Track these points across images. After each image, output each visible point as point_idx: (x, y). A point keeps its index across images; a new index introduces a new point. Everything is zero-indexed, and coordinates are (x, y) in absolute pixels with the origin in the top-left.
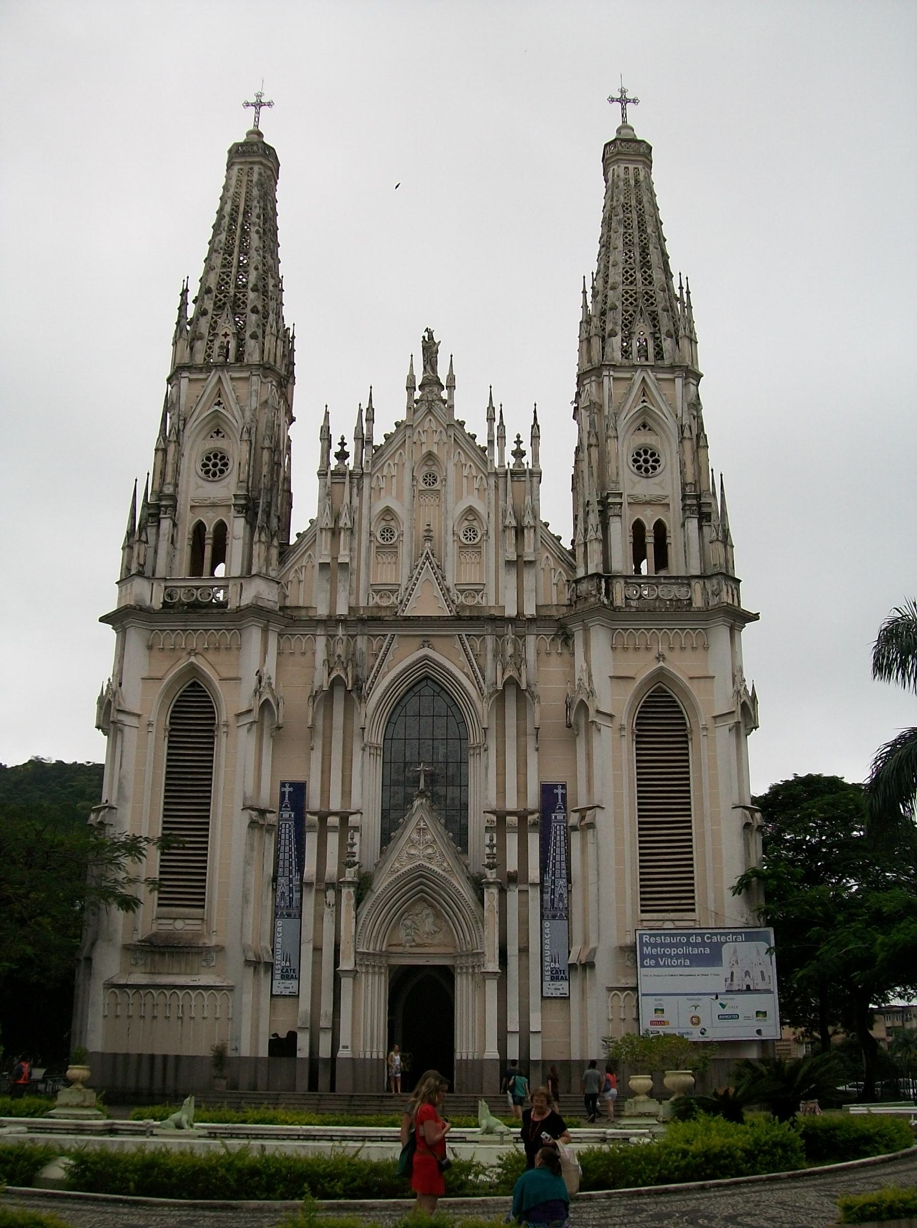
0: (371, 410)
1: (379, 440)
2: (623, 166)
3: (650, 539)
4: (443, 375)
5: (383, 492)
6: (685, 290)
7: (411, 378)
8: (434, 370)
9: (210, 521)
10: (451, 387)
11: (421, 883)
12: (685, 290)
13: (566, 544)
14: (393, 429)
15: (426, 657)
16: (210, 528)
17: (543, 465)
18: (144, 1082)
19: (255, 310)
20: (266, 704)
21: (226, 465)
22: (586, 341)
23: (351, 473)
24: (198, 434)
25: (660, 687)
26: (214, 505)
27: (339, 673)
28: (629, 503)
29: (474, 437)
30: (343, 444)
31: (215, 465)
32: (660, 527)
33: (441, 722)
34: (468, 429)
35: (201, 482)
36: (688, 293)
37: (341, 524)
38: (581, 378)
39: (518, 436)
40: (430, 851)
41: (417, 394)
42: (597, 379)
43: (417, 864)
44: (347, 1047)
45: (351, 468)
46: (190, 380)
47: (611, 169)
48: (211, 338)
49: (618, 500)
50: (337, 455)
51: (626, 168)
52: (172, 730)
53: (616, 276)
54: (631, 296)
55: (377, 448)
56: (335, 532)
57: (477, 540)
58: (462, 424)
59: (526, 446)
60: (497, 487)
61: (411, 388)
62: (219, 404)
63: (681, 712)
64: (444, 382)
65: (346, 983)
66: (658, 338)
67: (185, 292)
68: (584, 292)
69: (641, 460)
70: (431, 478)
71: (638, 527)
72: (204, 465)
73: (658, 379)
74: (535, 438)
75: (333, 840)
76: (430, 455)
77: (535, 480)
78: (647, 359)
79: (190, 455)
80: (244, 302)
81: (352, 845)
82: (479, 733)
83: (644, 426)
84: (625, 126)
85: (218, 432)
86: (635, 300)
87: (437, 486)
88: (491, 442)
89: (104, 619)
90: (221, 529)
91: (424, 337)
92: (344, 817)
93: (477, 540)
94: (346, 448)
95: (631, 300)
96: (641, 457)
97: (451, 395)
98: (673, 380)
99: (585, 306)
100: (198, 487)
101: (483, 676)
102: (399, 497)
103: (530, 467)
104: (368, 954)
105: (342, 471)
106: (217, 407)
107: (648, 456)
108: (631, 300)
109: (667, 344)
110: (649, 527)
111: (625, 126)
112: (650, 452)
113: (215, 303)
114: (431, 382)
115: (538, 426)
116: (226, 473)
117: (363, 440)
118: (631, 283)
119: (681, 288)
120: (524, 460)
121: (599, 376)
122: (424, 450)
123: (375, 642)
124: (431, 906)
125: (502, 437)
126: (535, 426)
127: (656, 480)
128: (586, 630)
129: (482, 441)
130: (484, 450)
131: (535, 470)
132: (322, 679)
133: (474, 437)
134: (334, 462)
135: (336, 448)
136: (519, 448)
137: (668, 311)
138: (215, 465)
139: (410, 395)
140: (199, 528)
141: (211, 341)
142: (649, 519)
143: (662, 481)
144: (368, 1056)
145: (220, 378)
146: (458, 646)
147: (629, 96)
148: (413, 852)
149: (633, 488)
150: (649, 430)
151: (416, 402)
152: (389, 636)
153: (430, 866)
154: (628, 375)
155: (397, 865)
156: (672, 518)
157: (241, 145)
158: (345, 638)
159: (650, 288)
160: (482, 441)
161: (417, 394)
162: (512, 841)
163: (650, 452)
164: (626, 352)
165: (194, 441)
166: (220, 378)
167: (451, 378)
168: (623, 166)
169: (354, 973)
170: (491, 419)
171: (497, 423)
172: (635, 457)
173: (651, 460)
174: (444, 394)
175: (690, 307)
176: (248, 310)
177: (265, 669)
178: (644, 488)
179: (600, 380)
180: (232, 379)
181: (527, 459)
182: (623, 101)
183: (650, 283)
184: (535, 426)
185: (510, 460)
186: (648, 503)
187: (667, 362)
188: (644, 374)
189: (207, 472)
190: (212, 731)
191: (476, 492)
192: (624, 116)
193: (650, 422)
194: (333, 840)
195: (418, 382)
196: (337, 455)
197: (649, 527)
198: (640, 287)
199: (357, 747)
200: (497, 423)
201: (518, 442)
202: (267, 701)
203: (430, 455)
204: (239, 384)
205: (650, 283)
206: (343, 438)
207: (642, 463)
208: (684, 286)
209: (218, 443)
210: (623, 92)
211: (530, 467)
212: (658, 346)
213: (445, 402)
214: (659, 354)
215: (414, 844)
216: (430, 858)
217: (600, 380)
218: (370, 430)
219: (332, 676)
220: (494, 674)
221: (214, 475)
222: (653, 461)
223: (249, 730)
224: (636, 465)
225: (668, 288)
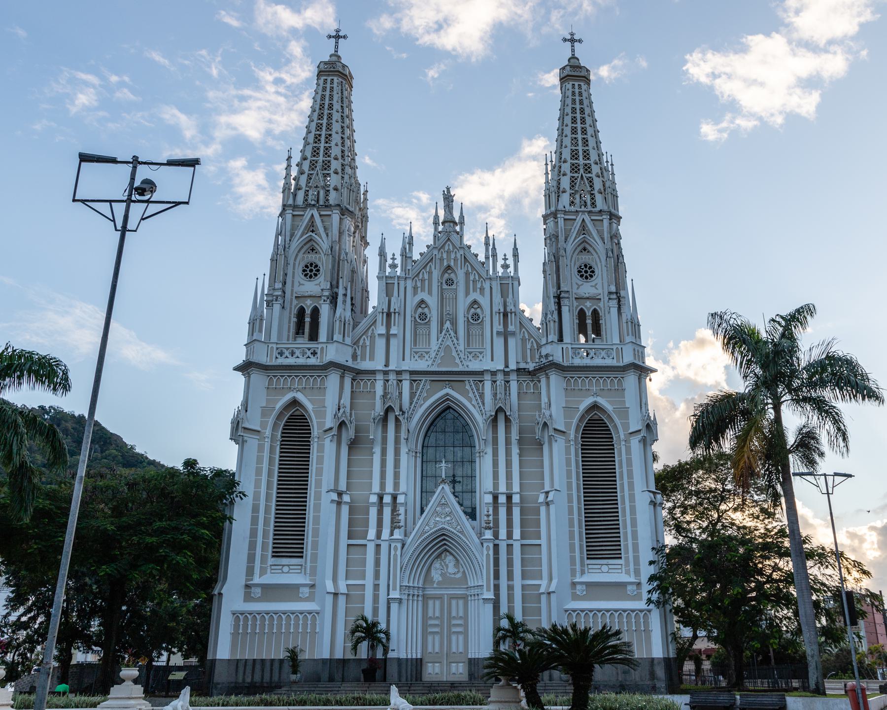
0: (411, 237)
1: (416, 256)
2: (571, 83)
3: (589, 321)
4: (456, 216)
5: (419, 289)
6: (610, 164)
7: (436, 217)
8: (451, 214)
9: (309, 305)
10: (462, 223)
11: (444, 539)
12: (610, 164)
13: (537, 323)
14: (425, 250)
15: (447, 394)
16: (308, 311)
17: (521, 274)
18: (257, 678)
19: (336, 173)
20: (342, 425)
21: (318, 270)
22: (548, 196)
23: (399, 277)
24: (299, 251)
25: (596, 414)
26: (310, 296)
27: (391, 404)
28: (576, 298)
29: (476, 256)
30: (393, 259)
31: (311, 271)
32: (595, 313)
33: (459, 436)
34: (473, 250)
35: (302, 282)
36: (612, 165)
37: (392, 310)
38: (545, 217)
39: (505, 255)
40: (448, 518)
41: (440, 228)
43: (440, 527)
44: (394, 650)
45: (398, 274)
46: (294, 216)
48: (307, 189)
49: (566, 295)
50: (390, 266)
51: (573, 84)
52: (283, 441)
53: (567, 154)
54: (576, 167)
55: (415, 262)
56: (389, 315)
57: (480, 321)
58: (469, 247)
59: (510, 262)
60: (491, 288)
61: (436, 223)
62: (313, 231)
63: (609, 430)
64: (457, 220)
65: (394, 607)
66: (593, 194)
67: (289, 158)
68: (547, 164)
70: (450, 282)
71: (582, 314)
72: (304, 271)
73: (592, 220)
74: (516, 255)
75: (387, 511)
76: (449, 267)
77: (516, 283)
79: (294, 264)
80: (329, 166)
81: (399, 515)
82: (482, 442)
83: (585, 249)
84: (573, 57)
85: (313, 250)
86: (579, 170)
87: (454, 287)
88: (487, 258)
89: (237, 369)
90: (316, 312)
91: (444, 191)
92: (394, 498)
93: (480, 321)
94: (396, 262)
95: (576, 169)
97: (461, 229)
99: (547, 173)
100: (300, 284)
101: (484, 404)
102: (430, 293)
103: (512, 274)
104: (409, 587)
105: (392, 275)
106: (311, 233)
108: (576, 169)
109: (599, 198)
110: (589, 313)
111: (573, 57)
113: (310, 166)
114: (449, 221)
115: (517, 249)
116: (319, 276)
117: (406, 255)
118: (576, 159)
119: (607, 162)
120: (508, 271)
121: (556, 218)
122: (445, 264)
123: (415, 385)
124: (451, 554)
125: (495, 256)
126: (515, 249)
127: (593, 284)
128: (548, 378)
129: (482, 258)
130: (483, 264)
131: (515, 276)
132: (379, 409)
133: (476, 256)
134: (388, 270)
135: (389, 262)
136: (505, 262)
137: (599, 177)
138: (311, 271)
139: (436, 229)
140: (301, 312)
141: (308, 191)
142: (588, 307)
143: (596, 284)
144: (409, 657)
145: (312, 215)
146: (468, 387)
148: (437, 519)
149: (578, 288)
151: (439, 232)
152: (423, 382)
153: (449, 528)
154: (574, 217)
155: (427, 528)
156: (601, 306)
157: (326, 63)
158: (395, 382)
159: (588, 162)
160: (482, 258)
161: (440, 228)
162: (502, 511)
164: (572, 203)
165: (297, 255)
166: (312, 215)
167: (462, 217)
169: (400, 601)
170: (487, 244)
171: (491, 247)
174: (458, 228)
175: (613, 174)
176: (331, 172)
177: (342, 402)
178: (587, 289)
180: (321, 216)
181: (511, 270)
182: (572, 41)
183: (588, 159)
184: (515, 249)
185: (500, 271)
186: (588, 298)
187: (598, 209)
188: (583, 216)
189: (306, 275)
190: (309, 442)
191: (478, 290)
192: (573, 50)
193: (588, 246)
194: (387, 511)
195: (441, 219)
196: (390, 266)
197: (589, 313)
198: (581, 161)
199: (404, 450)
200: (491, 247)
201: (505, 259)
202: (343, 421)
203: (449, 267)
204: (325, 218)
205: (588, 159)
206: (394, 255)
208: (609, 160)
209: (312, 257)
210: (572, 34)
211: (512, 274)
212: (593, 199)
213: (458, 233)
214: (594, 204)
215: (437, 514)
216: (449, 523)
218: (411, 250)
219: (386, 406)
220: (489, 406)
221: (311, 277)
223: (331, 441)
225: (599, 162)
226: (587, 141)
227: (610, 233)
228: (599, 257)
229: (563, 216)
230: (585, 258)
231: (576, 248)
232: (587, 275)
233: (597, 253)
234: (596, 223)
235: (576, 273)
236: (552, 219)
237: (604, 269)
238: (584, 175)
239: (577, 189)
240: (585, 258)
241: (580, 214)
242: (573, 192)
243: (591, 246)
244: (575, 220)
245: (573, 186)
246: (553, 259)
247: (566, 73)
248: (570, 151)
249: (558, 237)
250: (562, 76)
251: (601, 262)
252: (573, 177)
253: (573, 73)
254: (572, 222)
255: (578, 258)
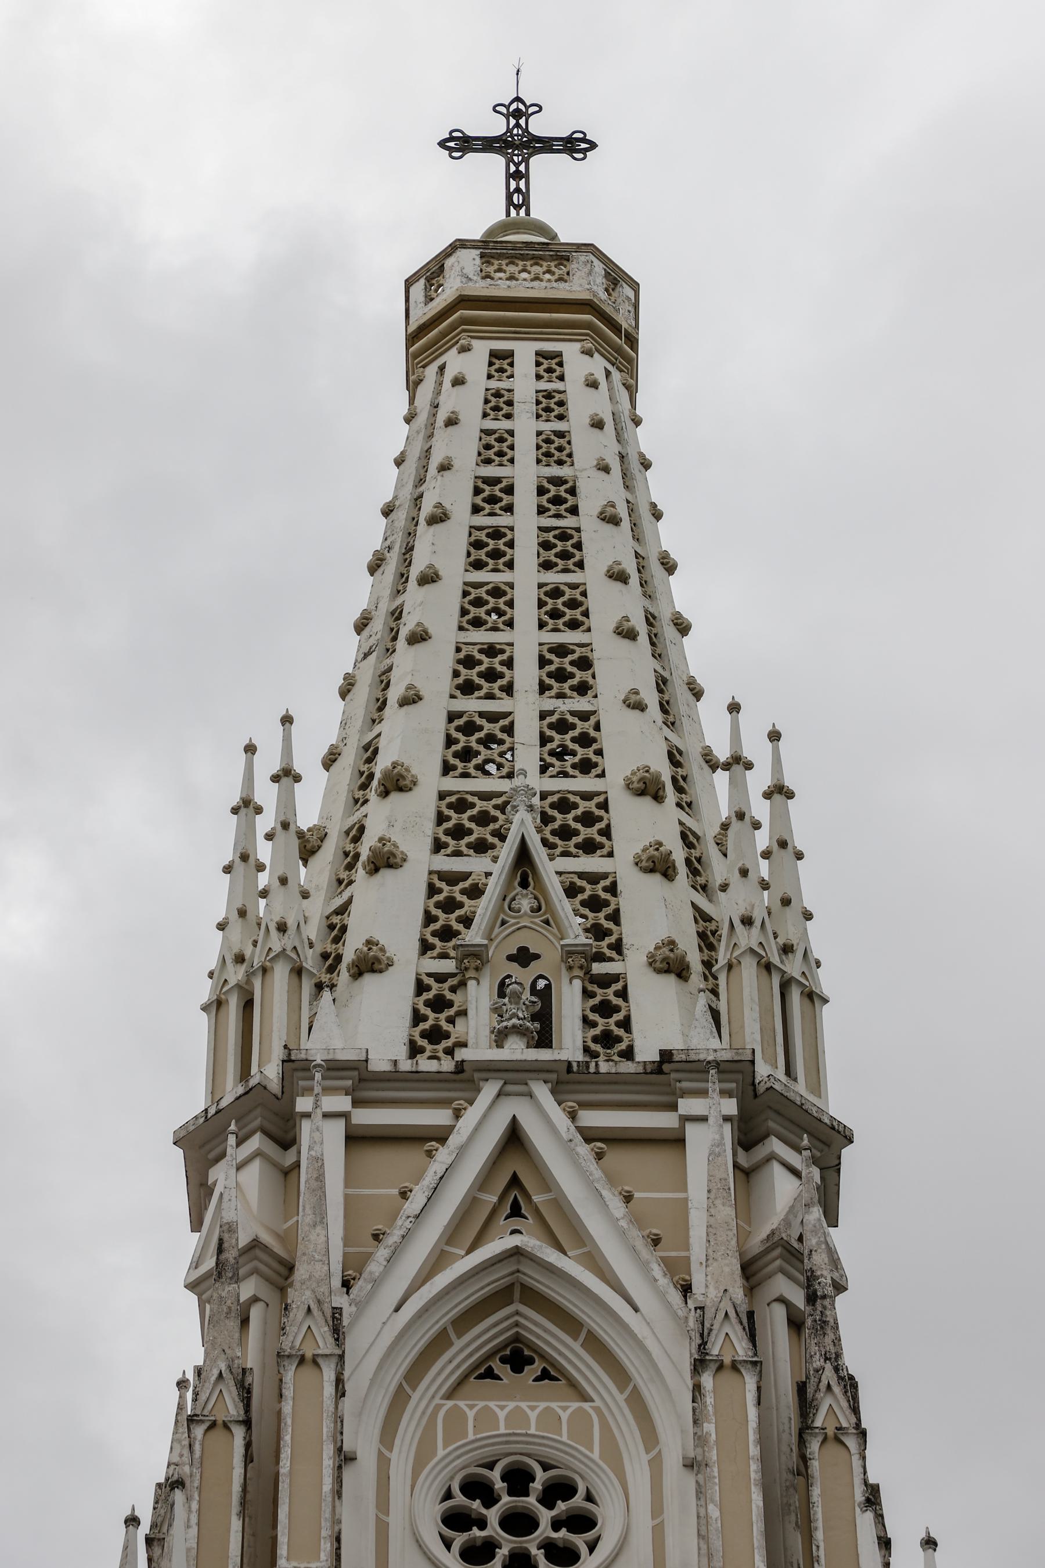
2: (482, 349)
42: (271, 1149)
47: (432, 370)
51: (494, 355)
69: (493, 1515)
73: (589, 1136)
78: (544, 1039)
95: (479, 832)
96: (490, 1499)
98: (676, 1141)
107: (532, 1500)
108: (479, 832)
112: (541, 1477)
147: (538, 127)
150: (545, 1375)
163: (541, 1477)
168: (482, 349)
172: (460, 1499)
173: (545, 1516)
179: (289, 1159)
207: (494, 1529)
217: (289, 1159)
222: (556, 1525)
224: (460, 1539)
226: (584, 663)
227: (743, 1236)
228: (638, 1404)
229: (343, 1103)
230: (517, 1417)
231: (439, 1344)
232: (532, 1544)
233: (620, 1374)
234: (619, 1158)
235: (431, 1530)
236: (256, 1142)
237: (676, 1478)
238: (539, 853)
239: (473, 936)
240: (517, 1417)
241: (489, 1091)
242: (448, 966)
243: (570, 1324)
244: (441, 1135)
245: (447, 934)
246: (232, 1408)
247: (451, 288)
248: (439, 726)
249: (291, 1268)
250: (421, 313)
251: (650, 1436)
252: (452, 878)
253: (502, 288)
254: (411, 1156)
255: (455, 1423)
